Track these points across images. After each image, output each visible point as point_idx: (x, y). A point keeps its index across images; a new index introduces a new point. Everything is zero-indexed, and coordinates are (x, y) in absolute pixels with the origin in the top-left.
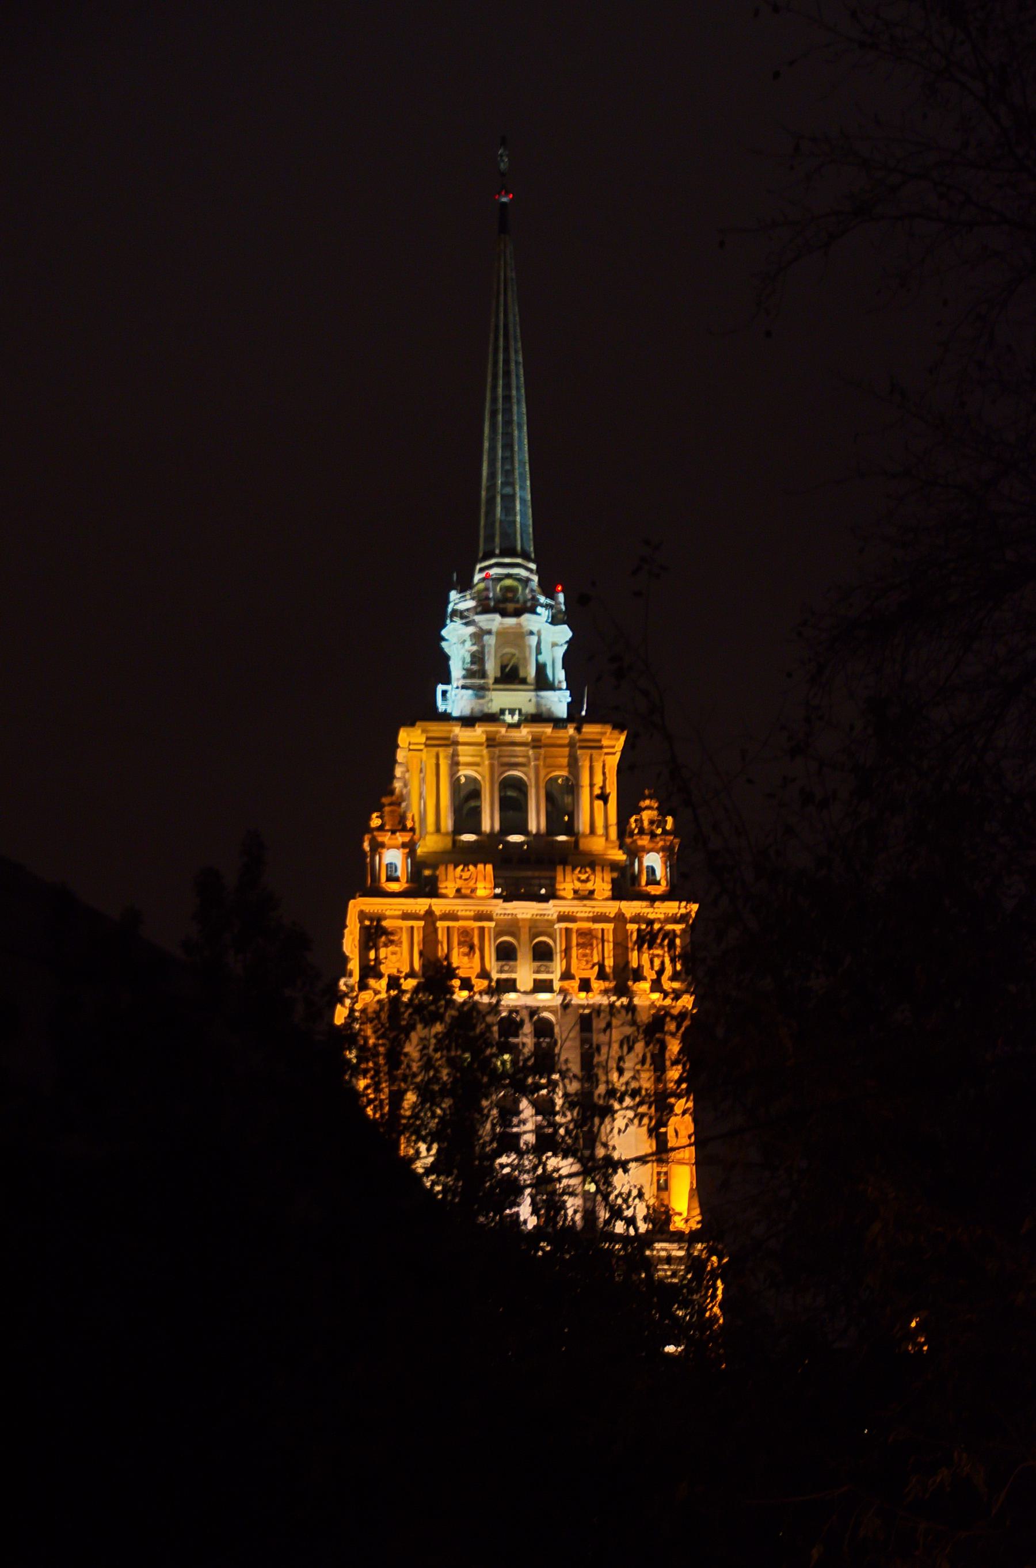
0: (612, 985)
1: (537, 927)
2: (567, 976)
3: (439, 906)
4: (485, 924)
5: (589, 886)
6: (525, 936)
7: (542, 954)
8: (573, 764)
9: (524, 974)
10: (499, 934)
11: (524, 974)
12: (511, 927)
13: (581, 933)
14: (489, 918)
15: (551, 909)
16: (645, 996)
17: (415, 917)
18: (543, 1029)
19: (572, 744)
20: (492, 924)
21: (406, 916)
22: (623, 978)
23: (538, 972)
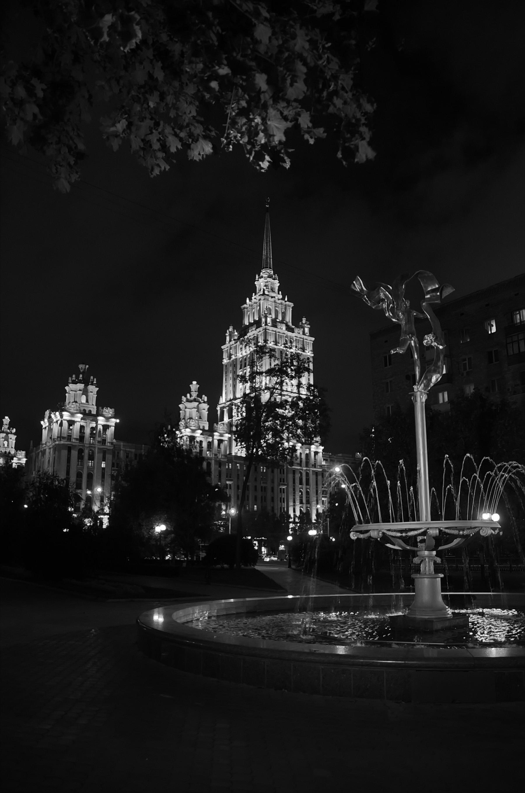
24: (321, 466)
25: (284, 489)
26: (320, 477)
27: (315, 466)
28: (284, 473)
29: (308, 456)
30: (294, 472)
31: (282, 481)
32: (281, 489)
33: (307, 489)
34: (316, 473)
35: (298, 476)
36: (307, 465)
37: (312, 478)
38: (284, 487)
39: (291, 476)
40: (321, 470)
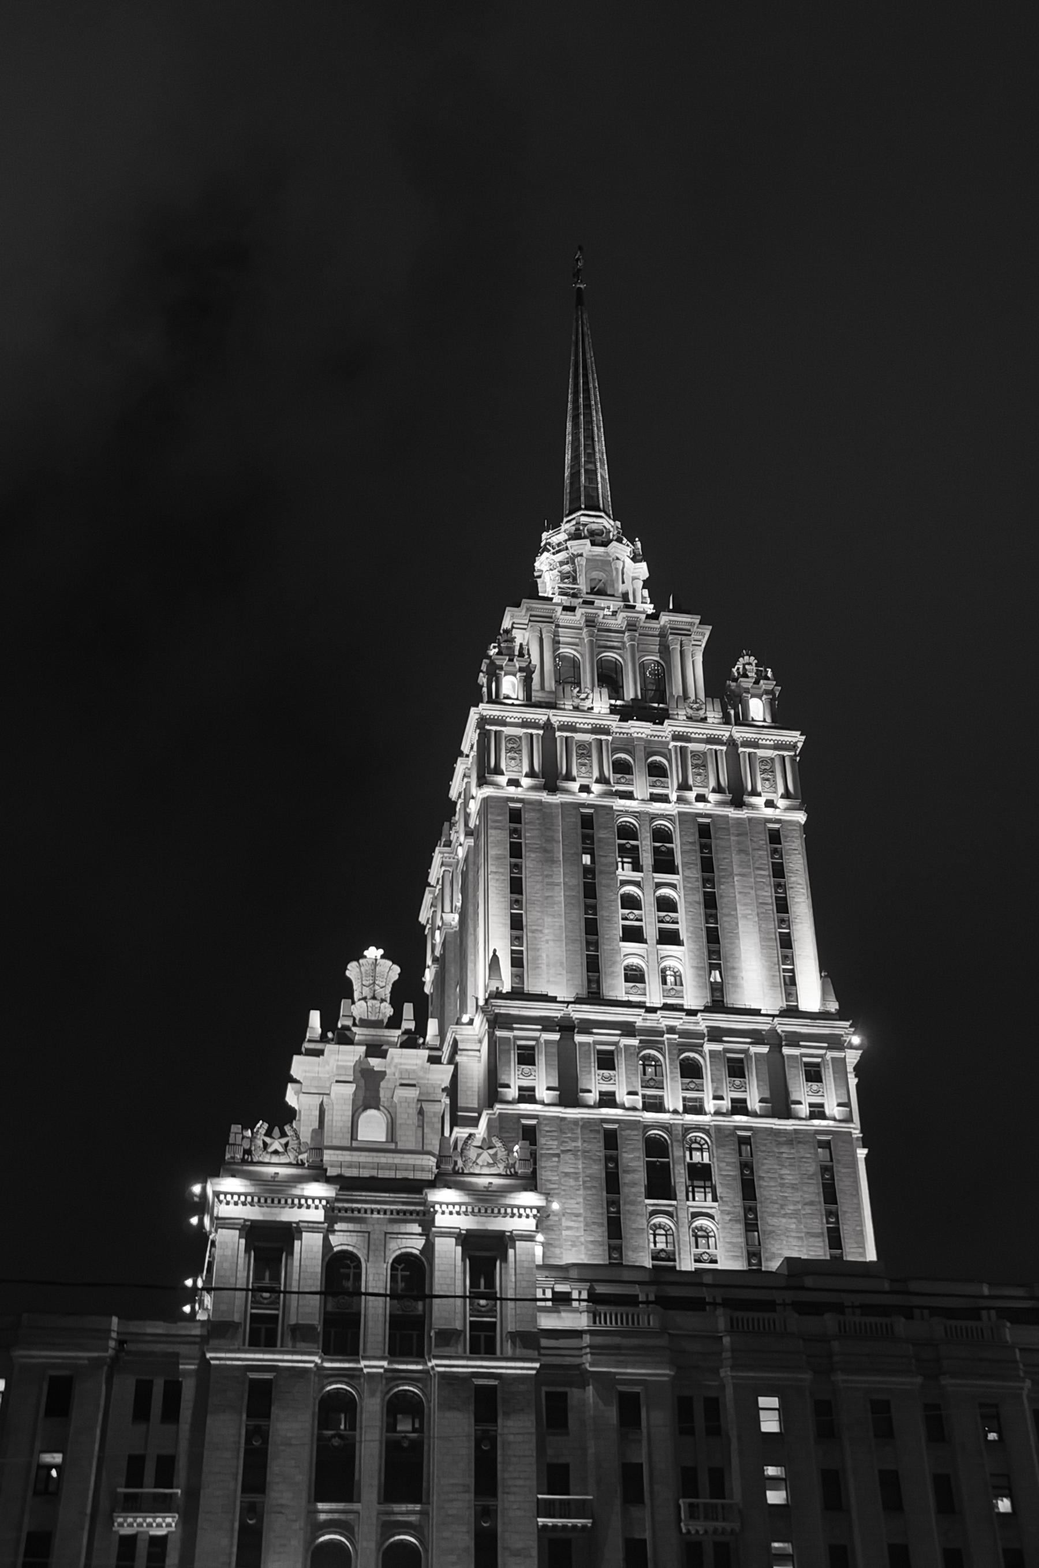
0: (729, 797)
1: (651, 747)
2: (684, 786)
3: (557, 718)
4: (603, 737)
5: (701, 713)
6: (640, 754)
7: (657, 772)
8: (665, 651)
9: (641, 786)
10: (615, 751)
11: (641, 786)
12: (627, 745)
13: (695, 755)
14: (606, 731)
15: (668, 729)
16: (759, 807)
17: (534, 725)
18: (661, 835)
19: (662, 635)
20: (610, 738)
21: (525, 724)
22: (737, 794)
23: (653, 786)
24: (529, 1340)
25: (159, 1543)
26: (517, 1432)
27: (483, 1340)
28: (171, 1413)
29: (413, 1272)
30: (261, 1395)
31: (148, 1478)
32: (129, 1542)
33: (389, 1527)
34: (486, 1401)
35: (293, 1429)
36: (409, 1335)
37: (450, 1436)
38: (163, 1525)
39: (227, 1430)
40: (528, 1368)
